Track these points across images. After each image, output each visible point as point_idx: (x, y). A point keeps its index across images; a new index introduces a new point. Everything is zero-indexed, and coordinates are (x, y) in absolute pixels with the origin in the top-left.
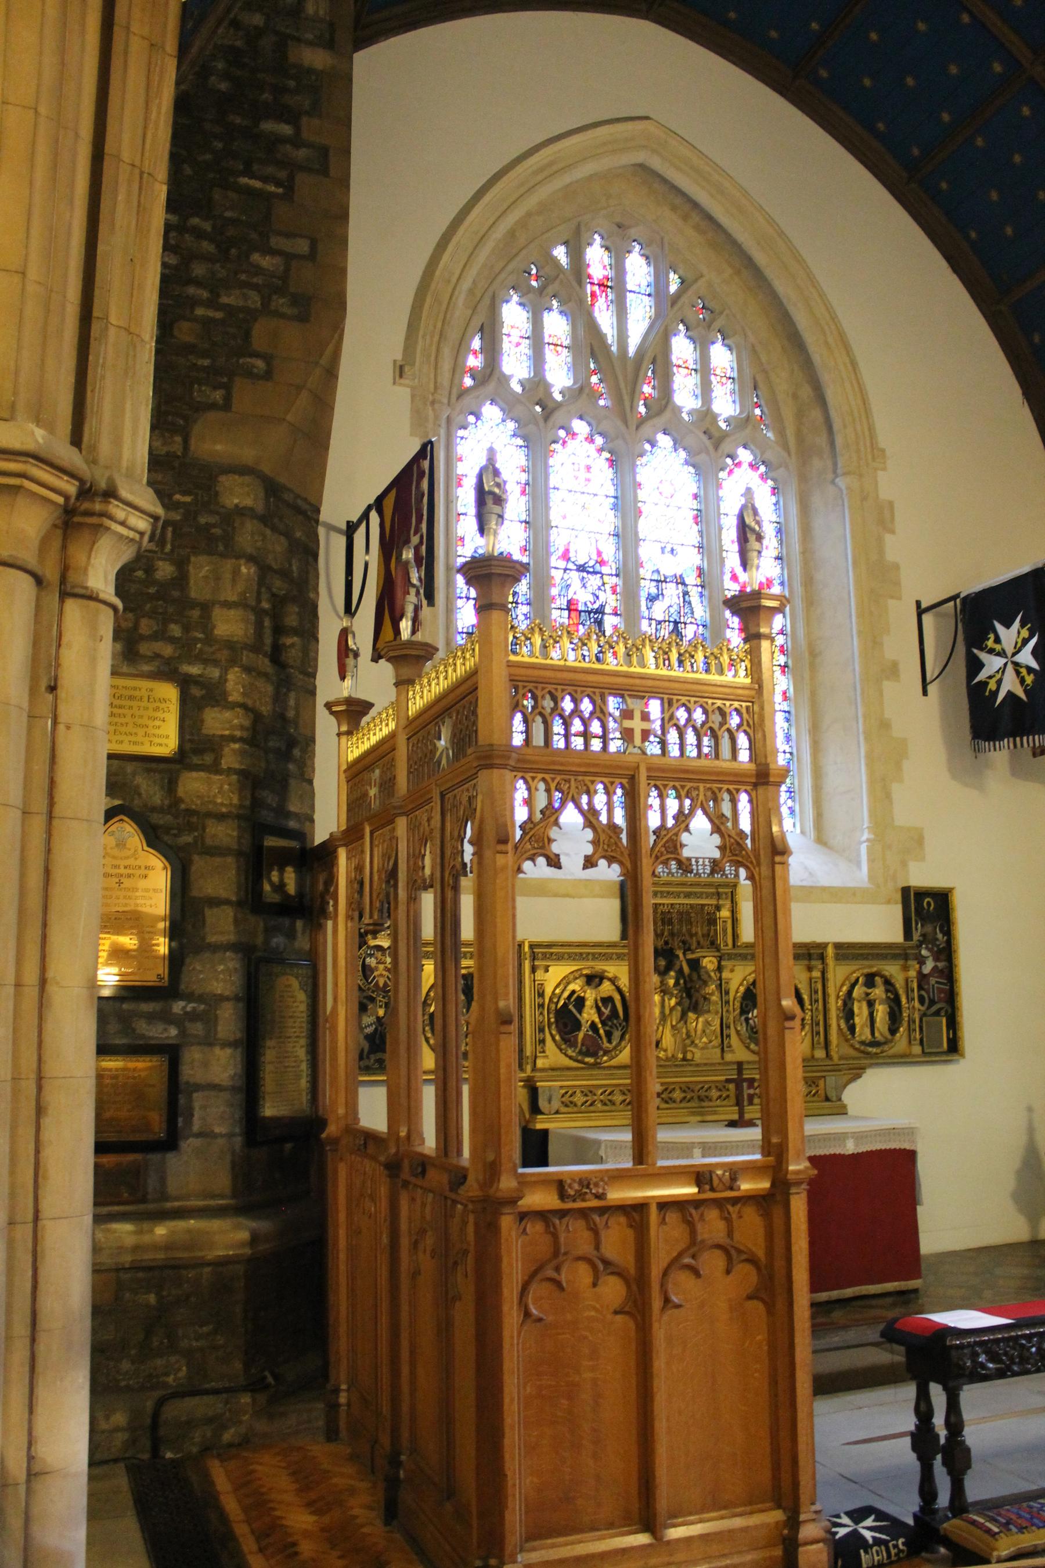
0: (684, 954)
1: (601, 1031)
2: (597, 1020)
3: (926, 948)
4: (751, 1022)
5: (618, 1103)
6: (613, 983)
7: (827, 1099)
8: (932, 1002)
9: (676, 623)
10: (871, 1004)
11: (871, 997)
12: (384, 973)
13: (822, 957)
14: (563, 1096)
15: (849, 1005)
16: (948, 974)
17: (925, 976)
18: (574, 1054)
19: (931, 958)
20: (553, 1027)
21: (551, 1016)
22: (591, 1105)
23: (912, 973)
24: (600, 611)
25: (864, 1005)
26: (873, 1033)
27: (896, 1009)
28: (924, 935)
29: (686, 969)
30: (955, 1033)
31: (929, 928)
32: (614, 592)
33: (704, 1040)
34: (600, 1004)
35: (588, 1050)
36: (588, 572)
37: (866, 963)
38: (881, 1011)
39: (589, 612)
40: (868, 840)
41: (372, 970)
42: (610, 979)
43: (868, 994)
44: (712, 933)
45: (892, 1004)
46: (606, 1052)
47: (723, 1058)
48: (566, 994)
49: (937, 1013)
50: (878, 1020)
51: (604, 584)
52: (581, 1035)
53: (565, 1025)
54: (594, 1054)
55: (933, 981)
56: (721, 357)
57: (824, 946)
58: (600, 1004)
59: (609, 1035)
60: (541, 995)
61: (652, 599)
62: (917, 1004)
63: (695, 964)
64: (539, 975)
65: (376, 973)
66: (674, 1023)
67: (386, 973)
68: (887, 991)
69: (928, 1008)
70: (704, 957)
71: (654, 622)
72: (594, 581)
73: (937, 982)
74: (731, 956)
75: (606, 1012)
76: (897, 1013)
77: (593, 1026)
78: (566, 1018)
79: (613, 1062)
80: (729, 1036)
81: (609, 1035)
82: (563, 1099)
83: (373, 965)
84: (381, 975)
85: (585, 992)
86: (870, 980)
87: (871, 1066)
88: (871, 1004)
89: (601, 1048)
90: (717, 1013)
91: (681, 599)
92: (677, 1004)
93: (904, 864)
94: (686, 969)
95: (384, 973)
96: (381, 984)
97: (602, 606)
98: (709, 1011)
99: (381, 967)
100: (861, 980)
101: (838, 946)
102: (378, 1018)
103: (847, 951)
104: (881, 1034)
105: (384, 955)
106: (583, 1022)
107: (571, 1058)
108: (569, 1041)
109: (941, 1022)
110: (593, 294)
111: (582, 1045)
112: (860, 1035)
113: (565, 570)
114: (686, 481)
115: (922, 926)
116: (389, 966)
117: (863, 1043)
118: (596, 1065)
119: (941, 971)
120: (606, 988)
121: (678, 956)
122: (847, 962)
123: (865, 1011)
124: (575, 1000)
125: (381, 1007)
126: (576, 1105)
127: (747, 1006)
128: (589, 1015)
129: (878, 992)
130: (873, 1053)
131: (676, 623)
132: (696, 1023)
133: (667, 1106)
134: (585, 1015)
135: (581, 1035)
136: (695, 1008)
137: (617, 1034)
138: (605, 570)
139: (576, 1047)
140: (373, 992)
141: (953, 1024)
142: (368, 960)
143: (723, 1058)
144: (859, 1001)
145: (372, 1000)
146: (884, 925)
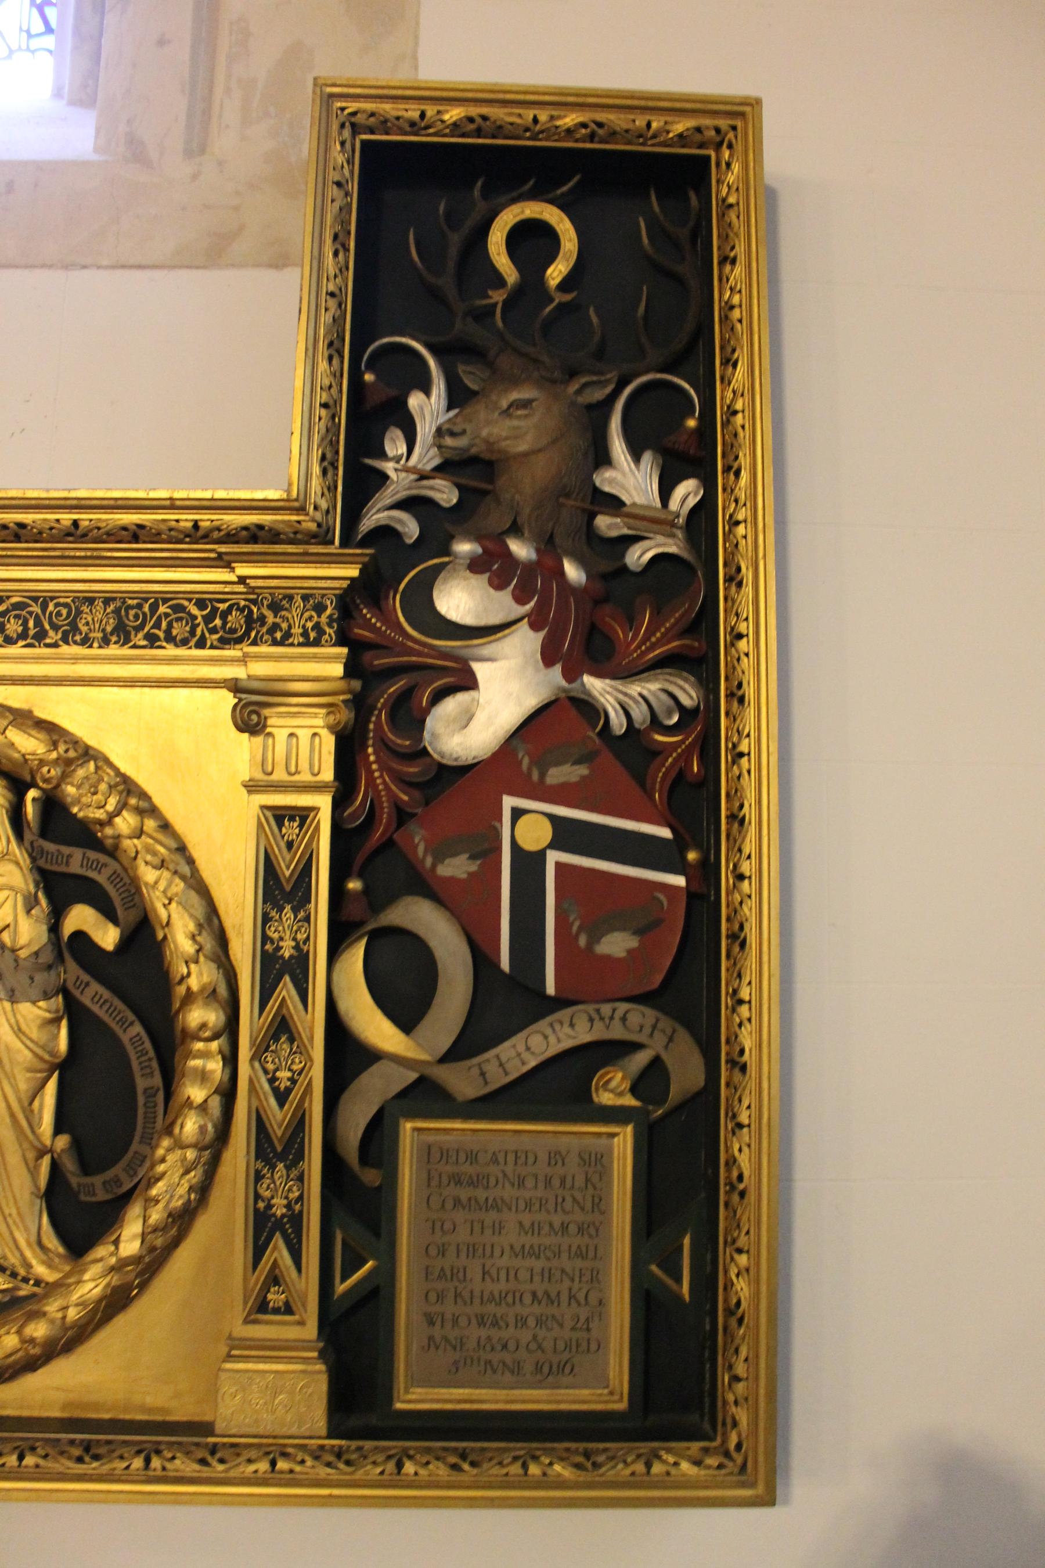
3: (495, 566)
8: (506, 999)
16: (685, 788)
17: (451, 775)
19: (524, 642)
31: (520, 424)
45: (94, 995)
49: (560, 1089)
68: (57, 890)
69: (462, 1049)
73: (565, 835)
76: (147, 1081)
119: (633, 748)
141: (693, 1175)
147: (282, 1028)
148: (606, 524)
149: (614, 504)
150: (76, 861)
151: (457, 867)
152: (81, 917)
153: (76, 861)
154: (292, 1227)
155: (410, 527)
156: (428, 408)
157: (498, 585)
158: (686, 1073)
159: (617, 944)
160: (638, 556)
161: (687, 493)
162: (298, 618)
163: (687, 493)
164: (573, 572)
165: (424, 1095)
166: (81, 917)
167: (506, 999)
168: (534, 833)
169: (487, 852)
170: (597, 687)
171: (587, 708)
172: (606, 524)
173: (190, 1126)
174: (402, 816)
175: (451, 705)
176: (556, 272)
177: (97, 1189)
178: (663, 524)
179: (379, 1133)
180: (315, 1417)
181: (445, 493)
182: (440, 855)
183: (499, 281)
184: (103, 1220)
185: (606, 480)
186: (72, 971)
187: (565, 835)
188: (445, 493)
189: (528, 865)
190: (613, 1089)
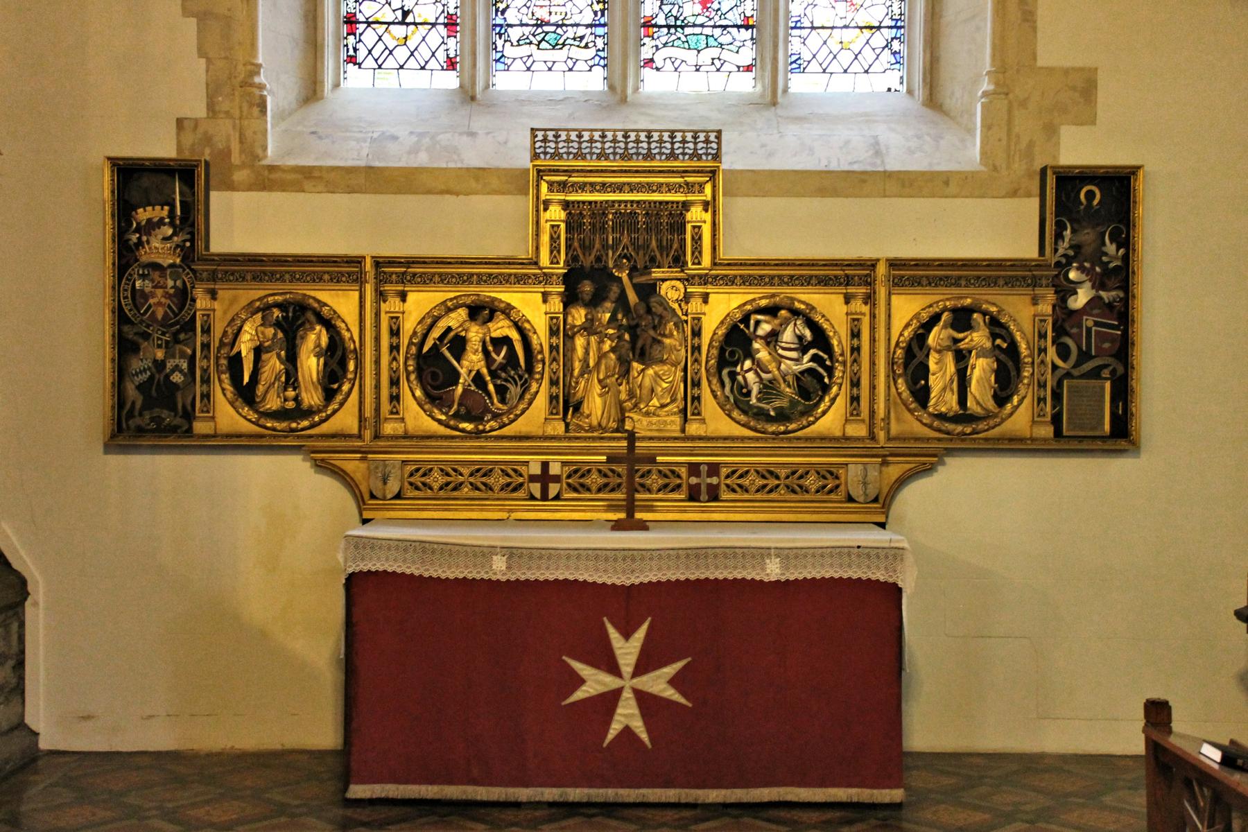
0: (630, 276)
1: (491, 387)
2: (485, 371)
3: (1081, 269)
4: (740, 378)
5: (496, 489)
6: (508, 316)
7: (850, 499)
8: (1084, 356)
10: (962, 357)
11: (962, 345)
12: (163, 300)
13: (869, 282)
14: (411, 475)
15: (920, 356)
16: (1120, 313)
17: (1073, 312)
18: (443, 417)
19: (1088, 285)
20: (413, 377)
21: (410, 362)
22: (455, 489)
23: (1046, 308)
25: (949, 358)
26: (962, 401)
27: (1010, 364)
28: (1076, 247)
29: (632, 297)
30: (1126, 409)
31: (1087, 236)
33: (655, 402)
34: (490, 348)
35: (468, 412)
37: (956, 291)
38: (981, 370)
40: (985, 94)
41: (146, 296)
42: (503, 312)
43: (956, 341)
44: (675, 246)
45: (1002, 357)
46: (496, 416)
47: (683, 430)
48: (436, 333)
49: (1095, 374)
50: (974, 382)
52: (460, 389)
53: (434, 376)
54: (478, 419)
55: (1088, 322)
57: (872, 264)
58: (490, 348)
59: (502, 391)
60: (395, 333)
62: (1052, 354)
63: (648, 291)
64: (393, 304)
65: (151, 301)
66: (601, 377)
67: (168, 302)
68: (994, 336)
70: (664, 280)
73: (1096, 324)
74: (704, 280)
75: (500, 358)
76: (1013, 373)
77: (478, 379)
78: (434, 367)
79: (506, 431)
80: (697, 399)
81: (502, 391)
82: (412, 480)
83: (147, 290)
84: (159, 304)
85: (466, 330)
86: (962, 319)
87: (950, 452)
88: (962, 357)
89: (490, 411)
90: (675, 365)
92: (613, 350)
93: (1051, 131)
94: (632, 297)
95: (163, 300)
96: (160, 317)
98: (662, 362)
99: (159, 292)
100: (945, 316)
101: (894, 264)
102: (155, 361)
103: (909, 274)
104: (978, 403)
105: (163, 276)
106: (463, 371)
107: (440, 422)
108: (440, 398)
109: (1103, 388)
111: (460, 405)
112: (936, 404)
115: (1074, 231)
116: (172, 291)
117: (941, 417)
118: (477, 434)
119: (1110, 306)
120: (501, 328)
121: (619, 280)
122: (919, 290)
123: (951, 368)
124: (450, 342)
125: (159, 346)
126: (431, 488)
127: (732, 354)
128: (473, 361)
129: (978, 337)
130: (966, 432)
132: (642, 374)
133: (575, 495)
134: (465, 363)
135: (460, 389)
136: (644, 356)
137: (514, 391)
139: (450, 407)
140: (148, 326)
141: (1123, 391)
142: (138, 284)
143: (683, 430)
144: (939, 352)
145: (146, 336)
146: (1007, 230)
147: (1042, 362)
148: (1105, 259)
149: (1106, 254)
150: (997, 330)
151: (1074, 330)
152: (998, 341)
153: (997, 330)
154: (1045, 399)
155: (1064, 261)
156: (1067, 233)
157: (1083, 272)
158: (1120, 370)
159: (1106, 345)
160: (1112, 265)
161: (1122, 251)
162: (1044, 282)
163: (1122, 251)
164: (1098, 269)
165: (1068, 375)
166: (998, 341)
167: (1084, 356)
168: (1090, 323)
169: (1080, 327)
170: (1102, 293)
171: (1100, 298)
172: (1105, 259)
173: (1026, 381)
174: (1064, 320)
175: (1073, 298)
176: (1095, 202)
177: (1004, 394)
178: (1116, 258)
179: (1060, 384)
180: (1052, 435)
181: (1071, 253)
182: (1072, 327)
183: (1081, 203)
184: (1008, 399)
185: (1104, 249)
186: (997, 352)
187: (1096, 324)
188: (1071, 253)
189: (1089, 330)
190: (1106, 373)
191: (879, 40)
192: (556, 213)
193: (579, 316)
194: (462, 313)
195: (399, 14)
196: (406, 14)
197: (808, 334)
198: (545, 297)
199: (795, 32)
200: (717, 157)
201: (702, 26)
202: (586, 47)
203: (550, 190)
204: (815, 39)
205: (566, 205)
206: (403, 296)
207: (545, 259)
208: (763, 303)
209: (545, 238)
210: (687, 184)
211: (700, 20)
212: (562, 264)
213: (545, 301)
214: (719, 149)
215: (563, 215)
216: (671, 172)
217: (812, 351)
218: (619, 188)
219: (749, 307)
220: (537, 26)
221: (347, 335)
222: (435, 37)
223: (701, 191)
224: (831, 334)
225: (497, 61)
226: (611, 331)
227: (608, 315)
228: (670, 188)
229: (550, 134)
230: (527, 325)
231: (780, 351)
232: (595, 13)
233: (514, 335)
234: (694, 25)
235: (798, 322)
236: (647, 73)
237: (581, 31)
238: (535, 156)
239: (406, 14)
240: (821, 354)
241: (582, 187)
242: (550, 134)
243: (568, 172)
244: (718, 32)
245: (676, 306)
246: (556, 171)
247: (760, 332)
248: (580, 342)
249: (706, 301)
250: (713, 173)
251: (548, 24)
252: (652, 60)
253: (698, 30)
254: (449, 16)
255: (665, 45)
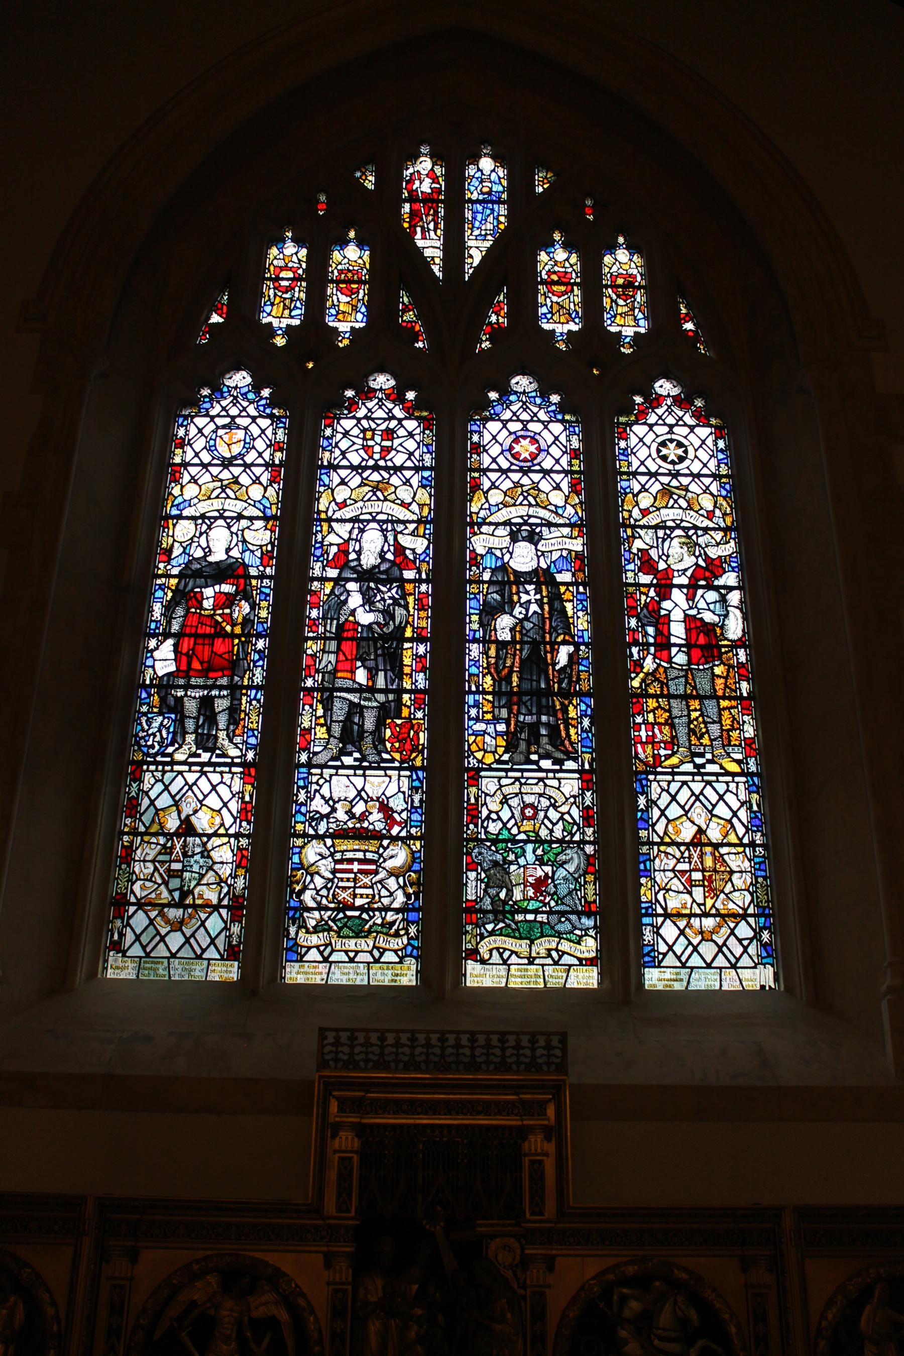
9: (535, 645)
24: (398, 636)
32: (421, 607)
36: (378, 581)
39: (375, 640)
51: (404, 596)
56: (622, 262)
61: (489, 612)
71: (493, 648)
72: (390, 593)
91: (546, 607)
97: (401, 629)
110: (413, 214)
113: (336, 581)
114: (556, 438)
120: (265, 1304)
131: (535, 645)
138: (409, 574)
191: (744, 931)
192: (346, 1140)
193: (374, 1289)
194: (213, 1280)
195: (176, 895)
196: (184, 894)
197: (693, 1315)
198: (329, 1260)
199: (646, 920)
200: (562, 1067)
201: (536, 912)
202: (397, 935)
203: (341, 1109)
204: (669, 931)
205: (361, 1130)
206: (133, 1256)
207: (330, 1205)
208: (631, 1270)
209: (332, 1175)
210: (523, 1102)
211: (533, 905)
212: (353, 1214)
213: (328, 1265)
214: (564, 1056)
215: (357, 1144)
216: (502, 1087)
217: (700, 1343)
218: (432, 1108)
219: (611, 1277)
220: (337, 910)
221: (51, 1311)
222: (214, 923)
223: (543, 1113)
224: (727, 1316)
225: (288, 950)
226: (419, 1312)
227: (415, 1287)
228: (501, 1108)
229: (344, 1036)
230: (301, 1302)
231: (656, 1342)
232: (408, 896)
233: (284, 1316)
234: (526, 911)
235: (680, 1299)
236: (472, 967)
237: (390, 917)
238: (323, 1064)
239: (184, 894)
240: (714, 1346)
241: (384, 1107)
242: (344, 1036)
243: (367, 1085)
244: (554, 918)
245: (509, 1274)
246: (350, 1084)
247: (627, 1313)
248: (374, 1327)
249: (551, 1268)
250: (557, 1089)
251: (353, 908)
252: (476, 951)
253: (530, 917)
254: (235, 898)
255: (492, 933)
